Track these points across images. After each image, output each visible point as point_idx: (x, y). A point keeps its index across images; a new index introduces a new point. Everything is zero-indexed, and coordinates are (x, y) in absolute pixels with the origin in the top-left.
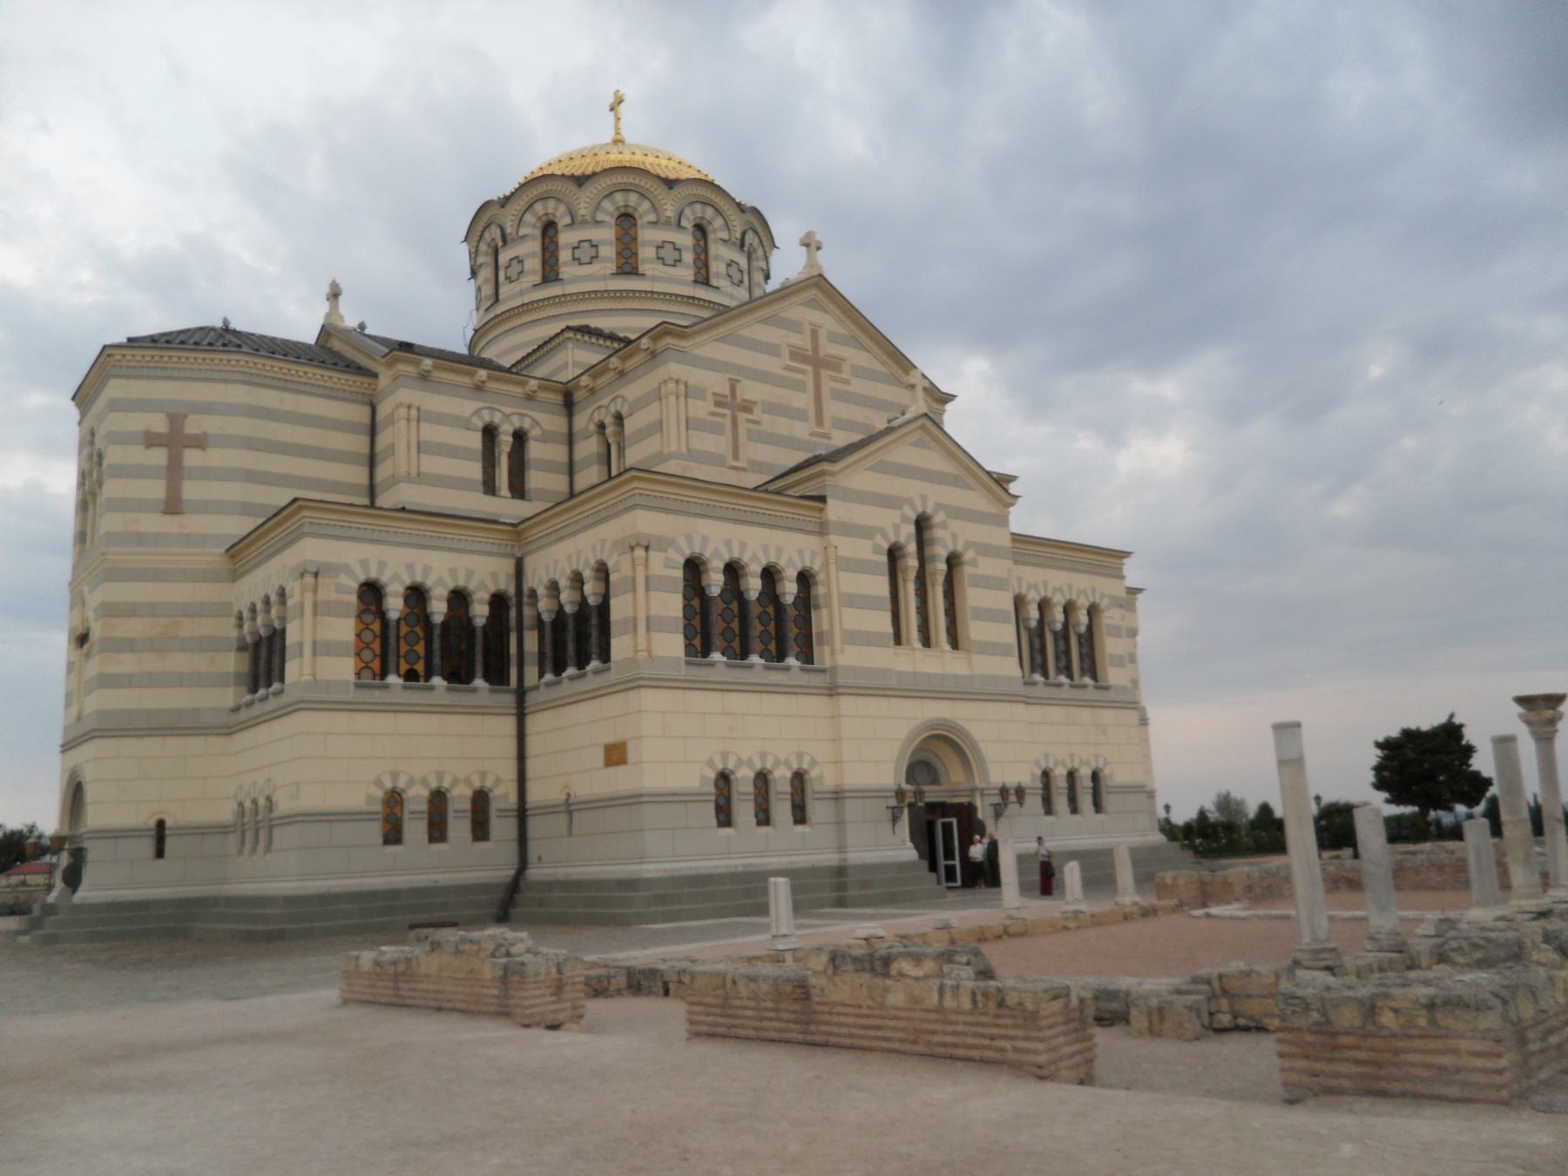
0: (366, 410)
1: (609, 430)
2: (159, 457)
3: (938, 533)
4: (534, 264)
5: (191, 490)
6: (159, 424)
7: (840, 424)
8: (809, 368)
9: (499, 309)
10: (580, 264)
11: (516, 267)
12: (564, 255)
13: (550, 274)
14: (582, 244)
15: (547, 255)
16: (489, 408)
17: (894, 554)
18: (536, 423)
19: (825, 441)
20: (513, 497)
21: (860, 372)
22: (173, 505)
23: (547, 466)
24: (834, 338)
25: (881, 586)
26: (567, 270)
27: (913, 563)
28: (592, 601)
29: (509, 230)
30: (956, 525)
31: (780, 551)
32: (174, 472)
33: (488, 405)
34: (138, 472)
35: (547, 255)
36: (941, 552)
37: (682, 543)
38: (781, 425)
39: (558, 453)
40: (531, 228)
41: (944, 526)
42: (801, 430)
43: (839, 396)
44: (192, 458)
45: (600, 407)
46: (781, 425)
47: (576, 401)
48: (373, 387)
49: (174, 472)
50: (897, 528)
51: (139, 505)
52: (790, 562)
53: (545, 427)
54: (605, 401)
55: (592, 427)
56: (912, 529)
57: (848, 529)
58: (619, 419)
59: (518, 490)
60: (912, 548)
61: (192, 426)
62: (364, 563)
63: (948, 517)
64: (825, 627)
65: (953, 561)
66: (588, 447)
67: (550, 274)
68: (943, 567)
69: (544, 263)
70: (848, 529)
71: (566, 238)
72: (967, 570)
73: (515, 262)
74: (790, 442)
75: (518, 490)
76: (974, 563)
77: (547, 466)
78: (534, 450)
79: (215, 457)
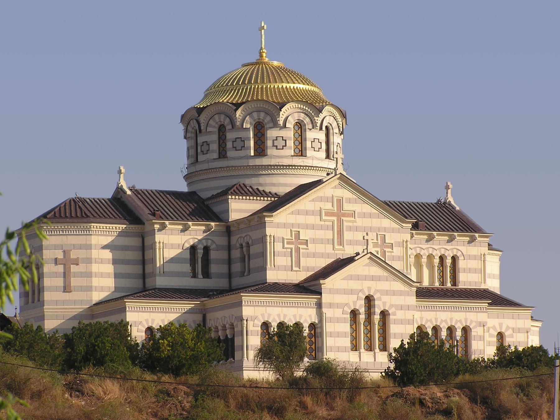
0: (140, 239)
1: (244, 249)
2: (60, 269)
3: (377, 303)
4: (214, 147)
5: (74, 282)
6: (60, 255)
7: (350, 243)
8: (335, 218)
9: (199, 167)
10: (236, 150)
11: (205, 148)
12: (229, 145)
13: (222, 154)
14: (237, 139)
15: (221, 141)
16: (192, 238)
17: (354, 314)
18: (213, 242)
19: (343, 252)
20: (204, 277)
21: (364, 215)
22: (66, 289)
23: (218, 262)
24: (349, 201)
25: (346, 327)
26: (230, 154)
27: (362, 317)
28: (229, 336)
29: (202, 128)
30: (385, 298)
31: (301, 316)
32: (66, 275)
33: (193, 237)
34: (55, 275)
35: (221, 141)
36: (378, 311)
37: (260, 317)
38: (320, 248)
39: (224, 255)
40: (213, 128)
41: (380, 299)
42: (329, 248)
43: (350, 229)
44: (74, 268)
45: (241, 237)
46: (320, 248)
47: (231, 230)
48: (143, 229)
49: (66, 275)
50: (354, 303)
51: (56, 289)
52: (306, 321)
53: (217, 243)
54: (243, 235)
55: (238, 245)
56: (363, 302)
57: (331, 305)
58: (248, 246)
59: (206, 274)
60: (362, 310)
61: (73, 255)
62: (147, 321)
63: (381, 295)
64: (320, 345)
65: (384, 314)
66: (236, 254)
67: (222, 154)
68: (377, 318)
69: (220, 146)
70: (331, 305)
71: (230, 135)
72: (391, 317)
73: (205, 144)
74: (322, 255)
75: (206, 274)
76: (395, 314)
77: (218, 262)
78: (213, 255)
79: (81, 268)
